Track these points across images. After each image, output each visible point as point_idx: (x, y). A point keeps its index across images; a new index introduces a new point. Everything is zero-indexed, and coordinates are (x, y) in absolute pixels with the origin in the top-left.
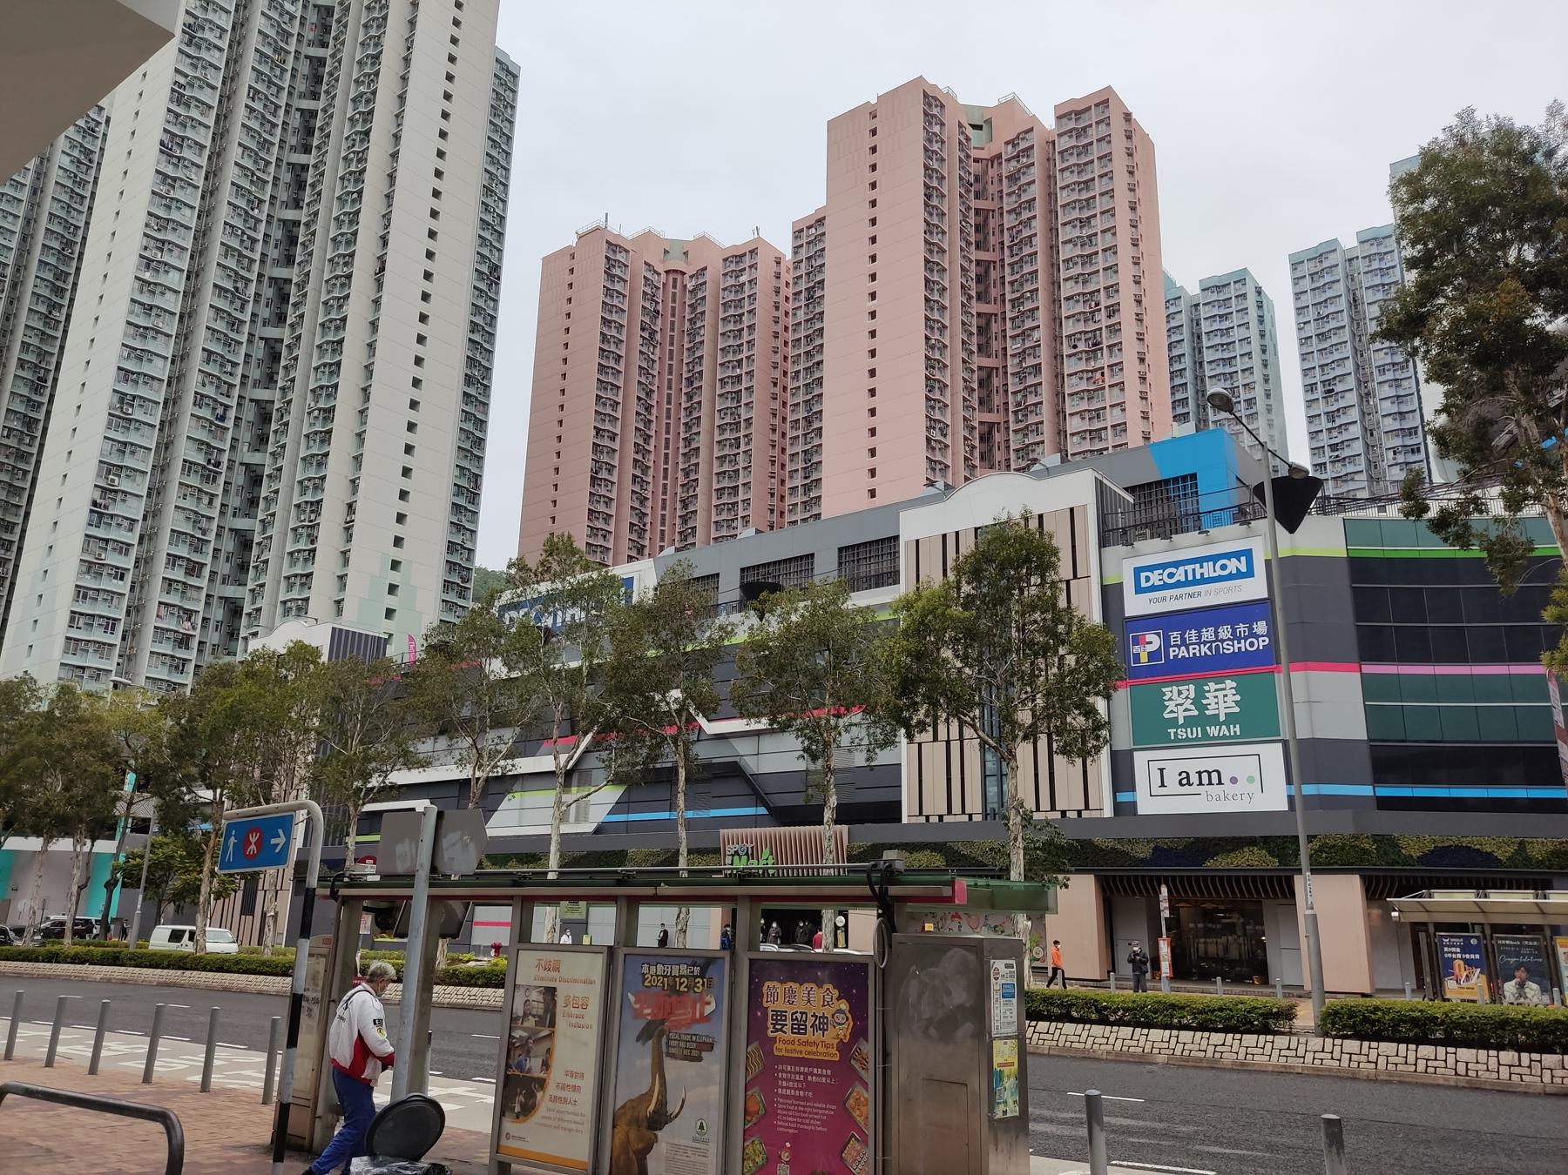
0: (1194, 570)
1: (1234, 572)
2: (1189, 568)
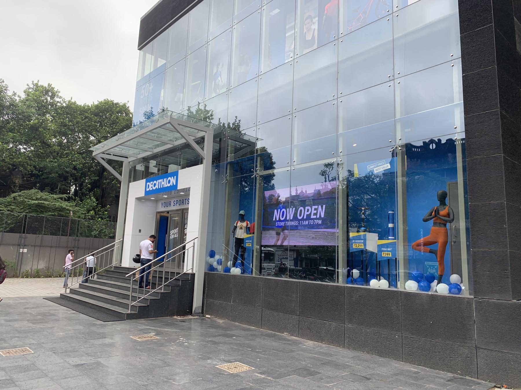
0: (161, 182)
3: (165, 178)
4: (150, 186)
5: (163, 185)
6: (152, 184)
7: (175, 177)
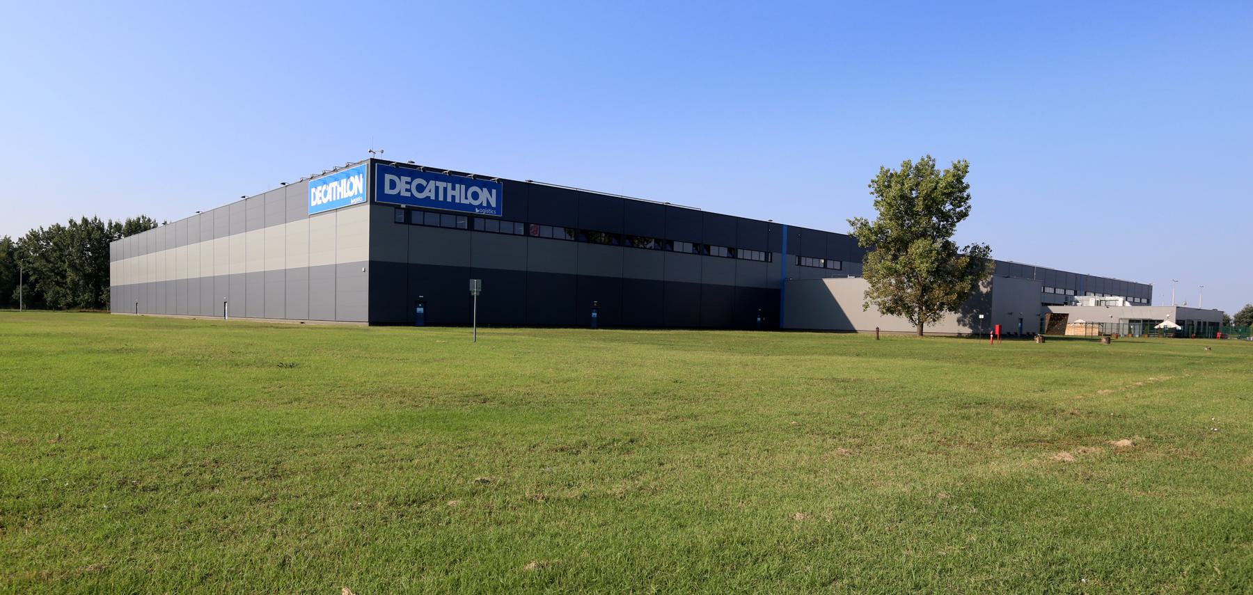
0: (445, 189)
1: (485, 204)
2: (441, 185)
5: (340, 193)
6: (321, 191)
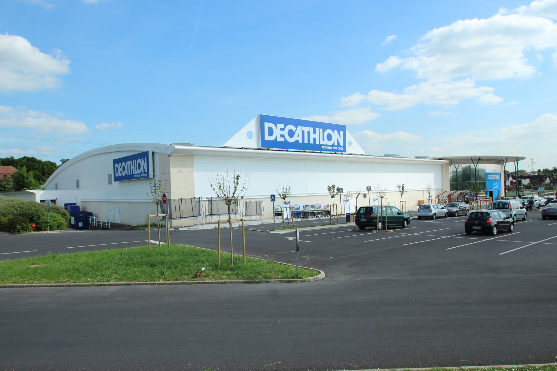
0: (309, 133)
1: (336, 144)
2: (306, 129)
3: (134, 160)
4: (120, 169)
5: (133, 170)
7: (146, 158)
